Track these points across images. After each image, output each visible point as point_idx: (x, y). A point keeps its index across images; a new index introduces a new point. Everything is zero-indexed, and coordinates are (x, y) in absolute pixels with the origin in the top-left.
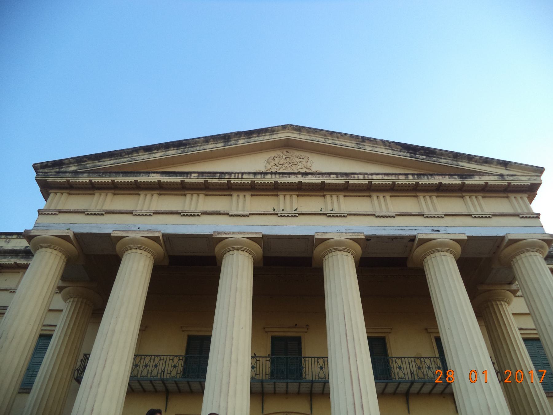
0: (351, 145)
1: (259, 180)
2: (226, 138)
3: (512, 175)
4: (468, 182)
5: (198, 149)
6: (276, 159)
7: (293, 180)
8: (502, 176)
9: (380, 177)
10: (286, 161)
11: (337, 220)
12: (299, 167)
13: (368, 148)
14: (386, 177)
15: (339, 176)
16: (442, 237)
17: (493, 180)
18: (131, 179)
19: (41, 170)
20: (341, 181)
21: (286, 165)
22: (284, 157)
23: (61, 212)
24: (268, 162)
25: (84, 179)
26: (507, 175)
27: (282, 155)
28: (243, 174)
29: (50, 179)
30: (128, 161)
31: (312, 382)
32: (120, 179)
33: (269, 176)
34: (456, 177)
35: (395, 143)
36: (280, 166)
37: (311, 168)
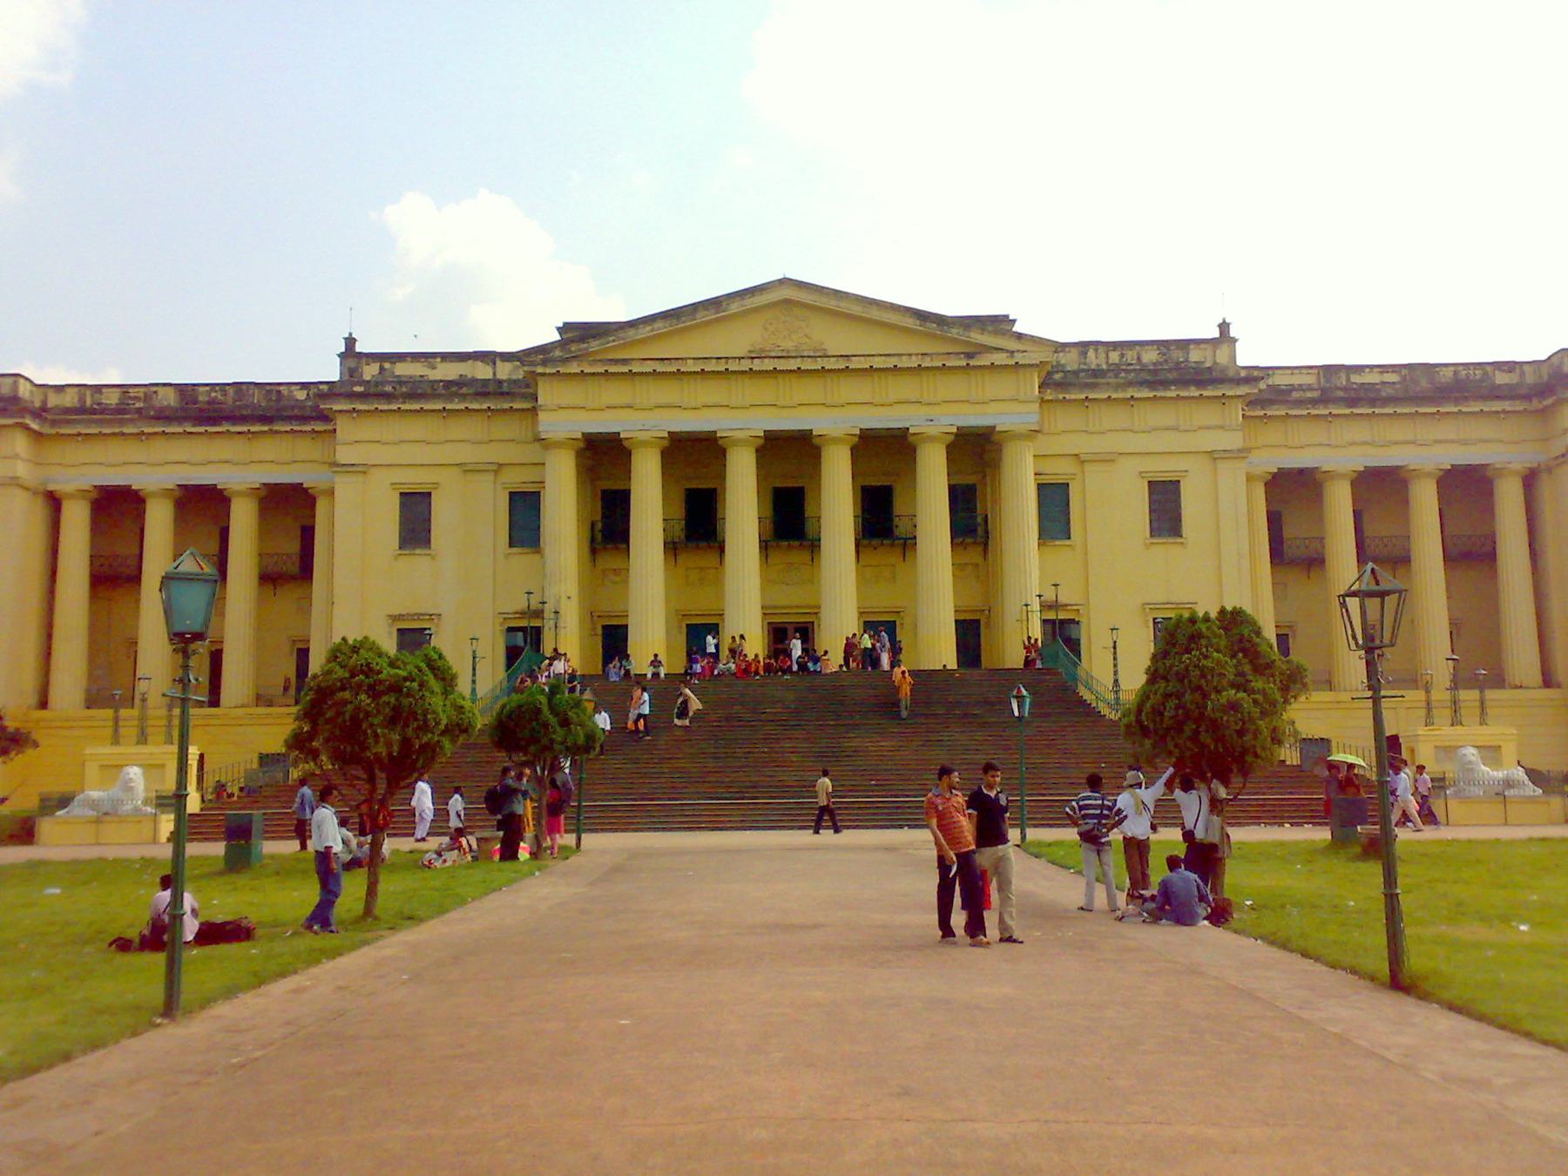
0: (856, 310)
1: (757, 365)
2: (715, 303)
4: (972, 363)
7: (792, 365)
11: (835, 412)
13: (875, 314)
14: (888, 359)
16: (931, 430)
17: (1000, 358)
18: (625, 369)
25: (574, 368)
29: (540, 370)
32: (612, 369)
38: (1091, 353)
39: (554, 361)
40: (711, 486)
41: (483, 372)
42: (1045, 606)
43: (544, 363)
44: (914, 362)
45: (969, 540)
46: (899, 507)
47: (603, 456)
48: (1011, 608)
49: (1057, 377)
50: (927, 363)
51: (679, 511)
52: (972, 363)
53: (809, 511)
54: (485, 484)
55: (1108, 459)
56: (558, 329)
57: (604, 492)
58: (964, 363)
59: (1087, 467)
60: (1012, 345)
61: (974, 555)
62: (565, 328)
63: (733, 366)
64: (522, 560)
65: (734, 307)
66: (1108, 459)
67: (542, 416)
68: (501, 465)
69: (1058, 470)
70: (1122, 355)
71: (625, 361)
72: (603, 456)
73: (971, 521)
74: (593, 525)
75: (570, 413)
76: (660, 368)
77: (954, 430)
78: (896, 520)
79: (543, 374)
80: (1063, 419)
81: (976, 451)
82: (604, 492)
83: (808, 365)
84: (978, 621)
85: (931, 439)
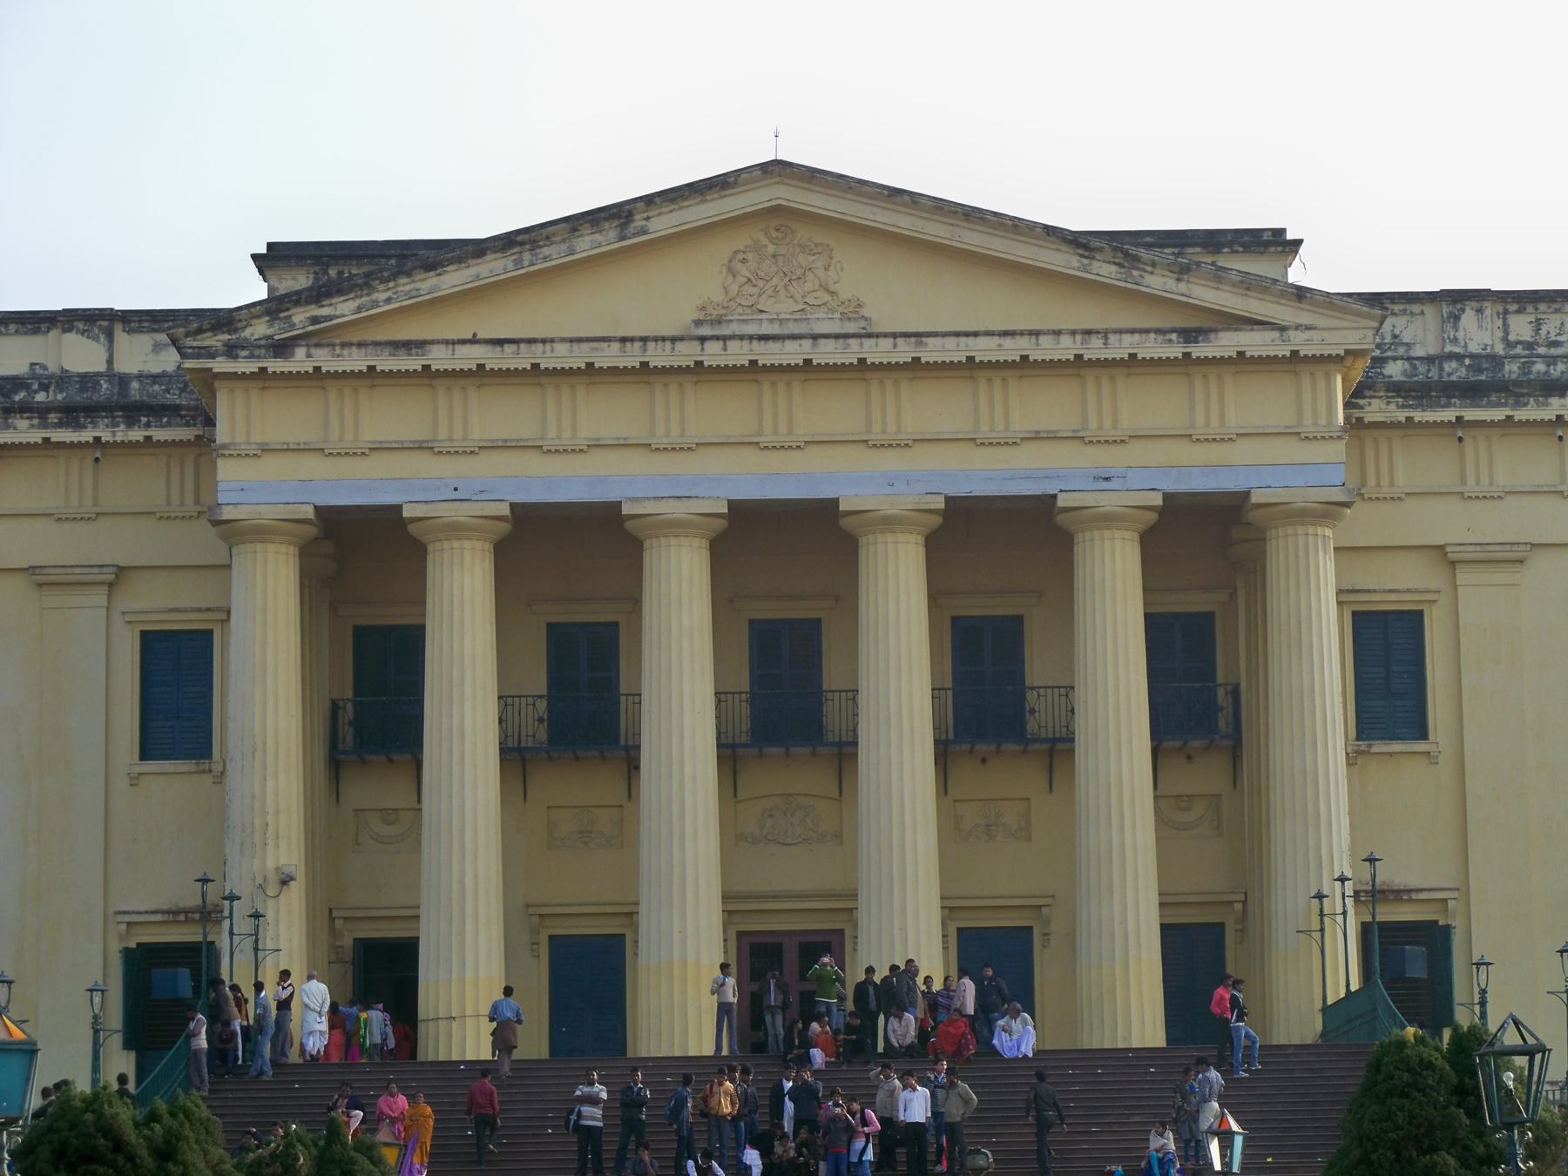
1: (713, 354)
2: (618, 215)
3: (1308, 328)
4: (1198, 351)
5: (555, 254)
6: (750, 256)
7: (792, 353)
8: (1283, 329)
9: (996, 340)
10: (774, 268)
12: (808, 286)
14: (1008, 342)
15: (900, 341)
16: (1108, 501)
17: (1255, 342)
18: (413, 363)
19: (189, 342)
20: (904, 352)
21: (774, 281)
22: (771, 249)
23: (265, 449)
24: (732, 272)
25: (300, 362)
26: (1298, 327)
27: (765, 241)
28: (674, 340)
29: (221, 365)
30: (388, 301)
31: (840, 744)
32: (386, 363)
33: (733, 346)
34: (1174, 336)
35: (1046, 227)
36: (761, 283)
37: (837, 288)
38: (1468, 318)
39: (252, 348)
40: (602, 618)
41: (81, 355)
42: (1372, 895)
43: (231, 351)
44: (1066, 349)
45: (1197, 743)
46: (1038, 670)
47: (361, 559)
48: (1287, 905)
49: (1395, 370)
50: (1095, 350)
51: (536, 681)
52: (1198, 351)
53: (832, 678)
54: (85, 615)
55: (1509, 558)
56: (255, 257)
57: (360, 633)
58: (1175, 351)
59: (1463, 576)
60: (1283, 313)
61: (1205, 776)
62: (273, 259)
63: (658, 357)
64: (172, 782)
65: (662, 223)
66: (1509, 558)
67: (227, 472)
68: (121, 571)
69: (1397, 582)
70: (1538, 325)
71: (408, 346)
72: (361, 559)
73: (1202, 703)
74: (335, 707)
75: (282, 461)
76: (495, 359)
77: (1157, 500)
78: (1031, 697)
79: (233, 376)
80: (1413, 465)
81: (1209, 547)
82: (360, 633)
83: (827, 353)
84: (1219, 928)
85: (1108, 520)
